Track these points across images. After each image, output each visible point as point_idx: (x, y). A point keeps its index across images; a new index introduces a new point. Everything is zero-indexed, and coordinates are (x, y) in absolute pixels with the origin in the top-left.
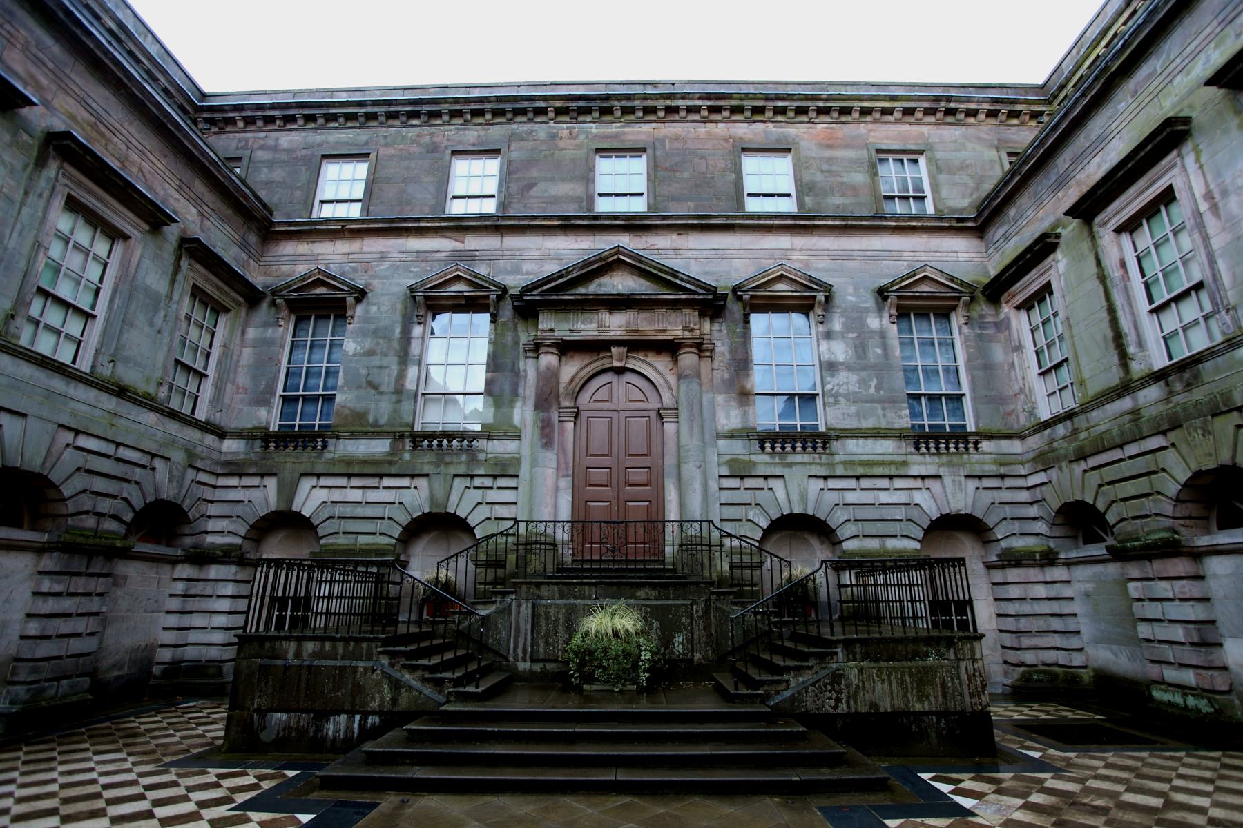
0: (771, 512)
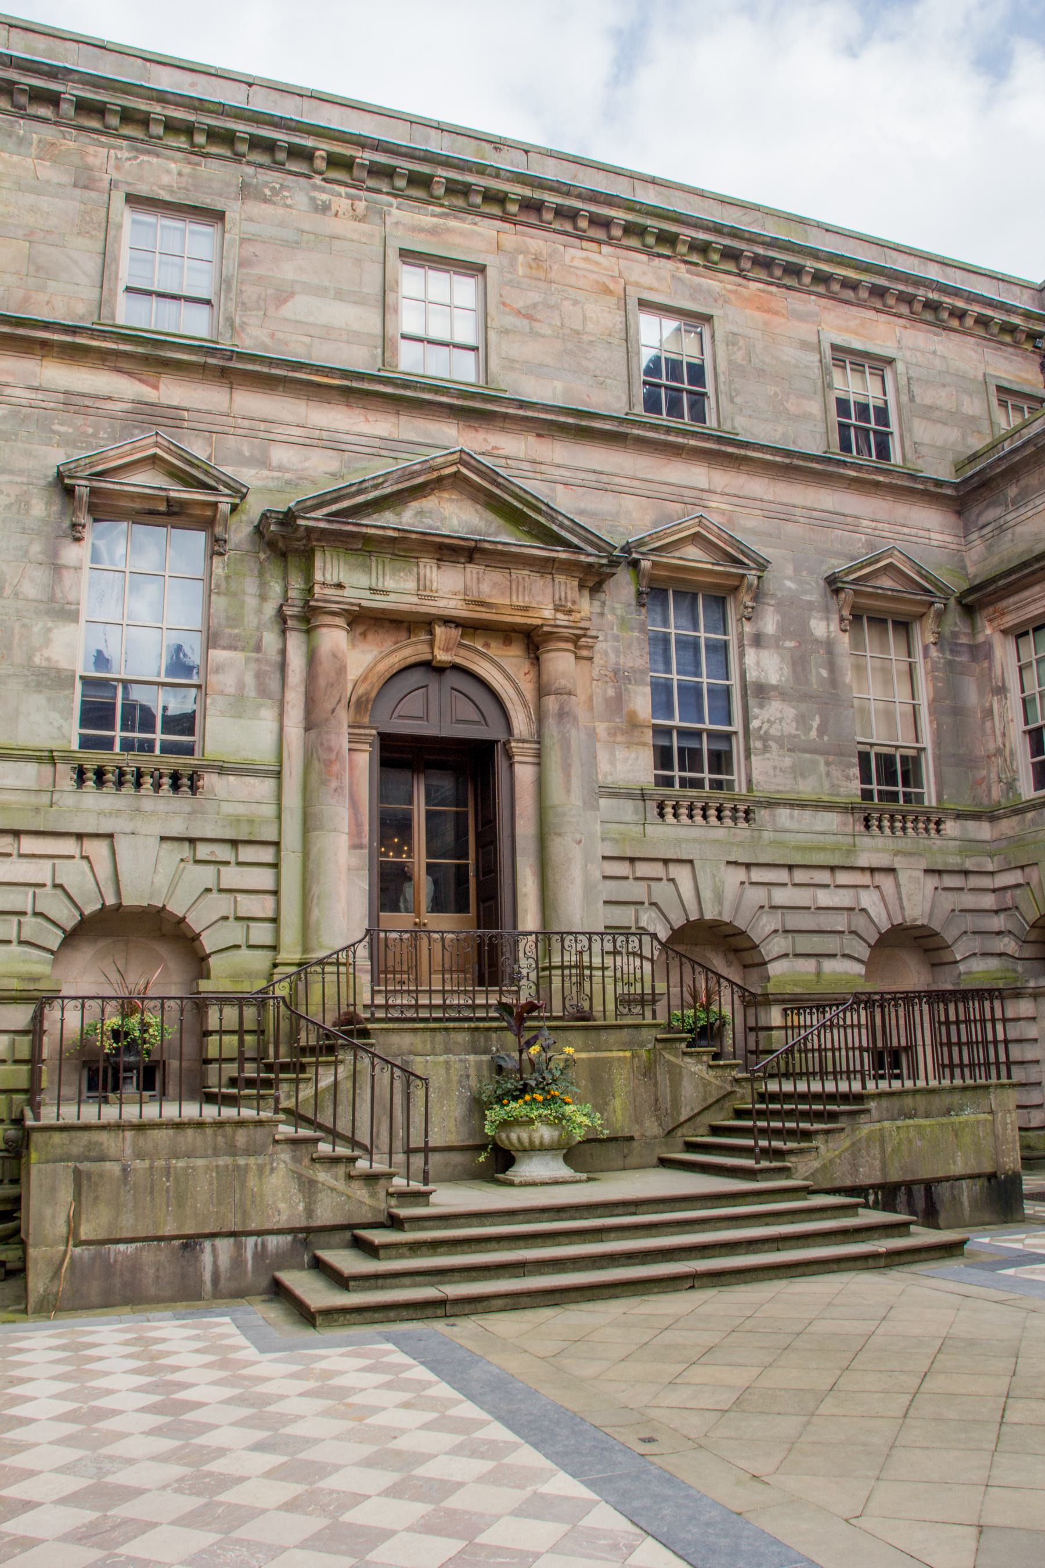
0: (672, 917)
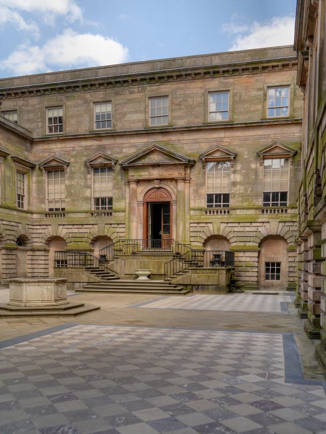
0: (208, 234)
